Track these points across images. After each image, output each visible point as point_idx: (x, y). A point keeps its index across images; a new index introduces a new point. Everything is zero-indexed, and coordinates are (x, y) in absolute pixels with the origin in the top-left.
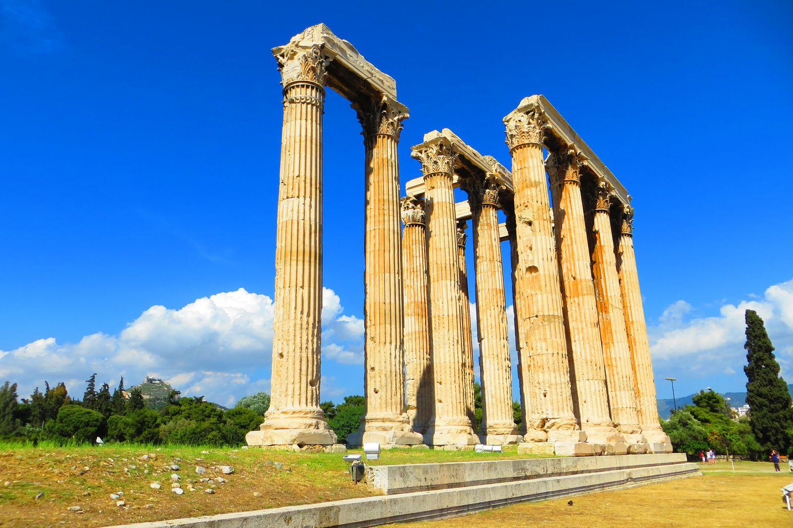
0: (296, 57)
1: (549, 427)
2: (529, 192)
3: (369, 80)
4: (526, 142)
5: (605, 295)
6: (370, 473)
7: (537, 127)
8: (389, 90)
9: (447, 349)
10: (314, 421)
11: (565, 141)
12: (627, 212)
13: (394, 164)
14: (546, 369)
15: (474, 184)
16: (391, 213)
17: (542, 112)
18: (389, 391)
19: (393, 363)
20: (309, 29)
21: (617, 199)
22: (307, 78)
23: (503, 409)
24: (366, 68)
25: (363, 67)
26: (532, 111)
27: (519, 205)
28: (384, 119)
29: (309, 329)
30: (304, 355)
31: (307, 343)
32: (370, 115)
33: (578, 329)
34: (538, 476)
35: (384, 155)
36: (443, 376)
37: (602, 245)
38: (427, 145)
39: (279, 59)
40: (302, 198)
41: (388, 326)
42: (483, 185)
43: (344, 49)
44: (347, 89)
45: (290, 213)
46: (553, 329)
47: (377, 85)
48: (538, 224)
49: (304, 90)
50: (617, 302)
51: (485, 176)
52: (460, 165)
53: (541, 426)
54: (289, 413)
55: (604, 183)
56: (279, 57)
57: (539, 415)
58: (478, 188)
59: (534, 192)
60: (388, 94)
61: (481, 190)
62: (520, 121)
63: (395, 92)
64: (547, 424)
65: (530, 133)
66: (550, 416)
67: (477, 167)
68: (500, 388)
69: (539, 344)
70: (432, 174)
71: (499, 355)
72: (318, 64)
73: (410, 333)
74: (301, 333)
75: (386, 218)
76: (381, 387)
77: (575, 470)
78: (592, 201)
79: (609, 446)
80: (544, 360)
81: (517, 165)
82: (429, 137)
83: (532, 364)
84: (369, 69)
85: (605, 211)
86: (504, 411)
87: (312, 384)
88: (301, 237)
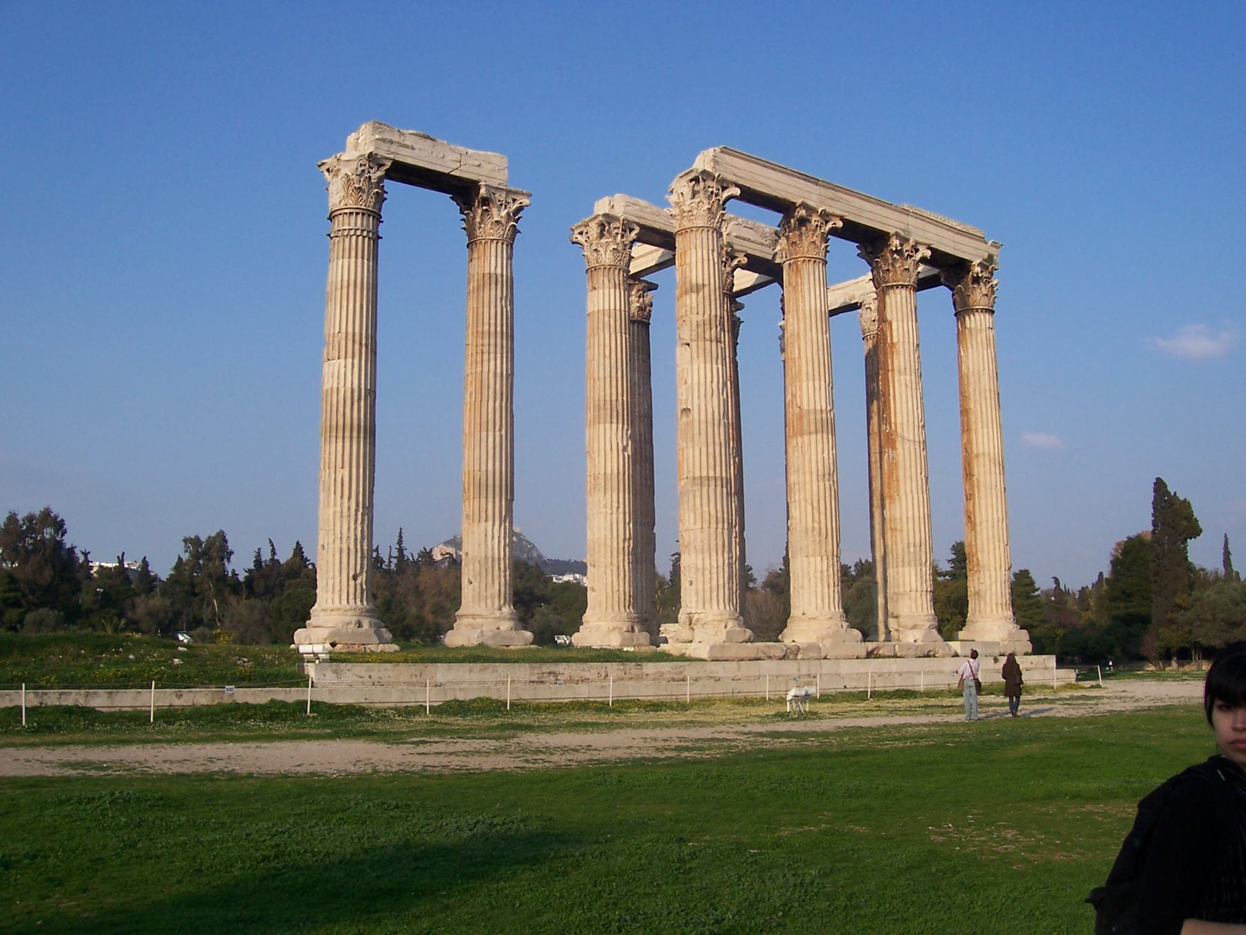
5: (893, 421)
9: (602, 520)
10: (355, 619)
13: (500, 279)
14: (692, 550)
16: (492, 349)
33: (799, 484)
36: (596, 557)
37: (895, 340)
40: (342, 360)
41: (483, 500)
74: (341, 522)
75: (486, 356)
76: (474, 576)
78: (883, 271)
80: (692, 537)
88: (341, 409)
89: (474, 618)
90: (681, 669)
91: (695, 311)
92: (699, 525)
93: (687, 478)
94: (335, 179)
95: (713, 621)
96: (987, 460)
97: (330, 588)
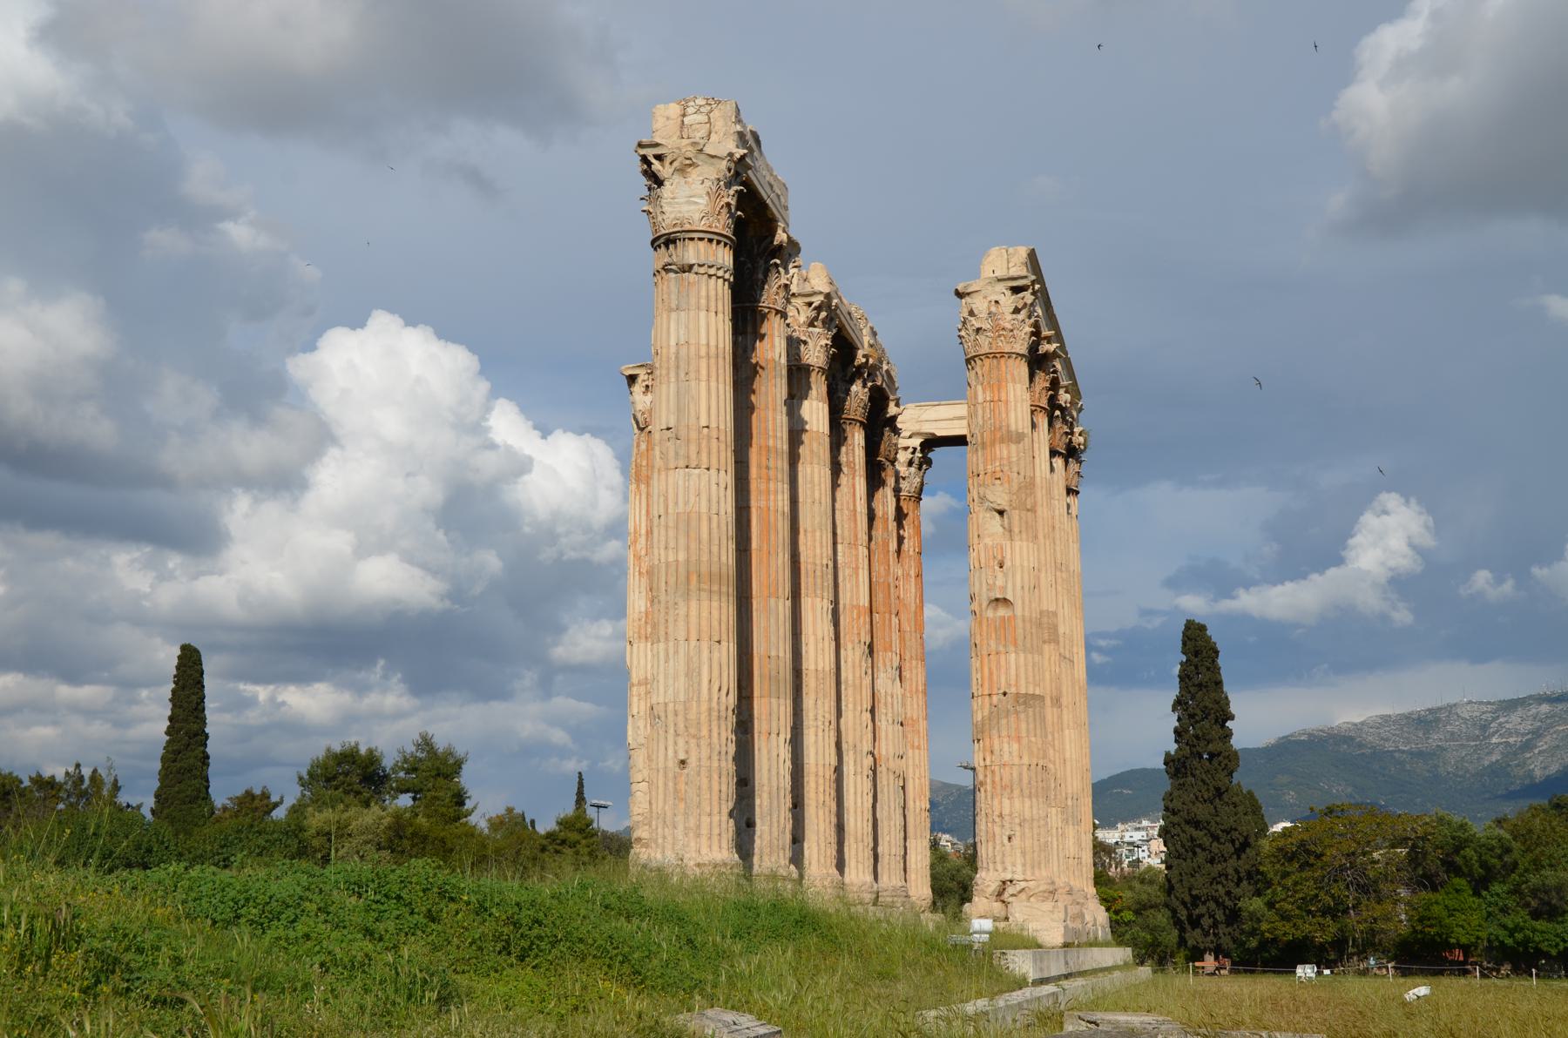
1: (1012, 895)
2: (1005, 453)
12: (1079, 445)
14: (1017, 792)
23: (860, 854)
27: (982, 473)
46: (1031, 719)
48: (1017, 517)
51: (854, 357)
56: (653, 161)
57: (996, 873)
59: (1014, 454)
62: (997, 302)
64: (1010, 890)
66: (1017, 877)
68: (856, 812)
69: (1006, 746)
71: (858, 745)
80: (1015, 775)
81: (984, 392)
93: (1005, 694)
94: (677, 178)
95: (1045, 892)
97: (704, 831)
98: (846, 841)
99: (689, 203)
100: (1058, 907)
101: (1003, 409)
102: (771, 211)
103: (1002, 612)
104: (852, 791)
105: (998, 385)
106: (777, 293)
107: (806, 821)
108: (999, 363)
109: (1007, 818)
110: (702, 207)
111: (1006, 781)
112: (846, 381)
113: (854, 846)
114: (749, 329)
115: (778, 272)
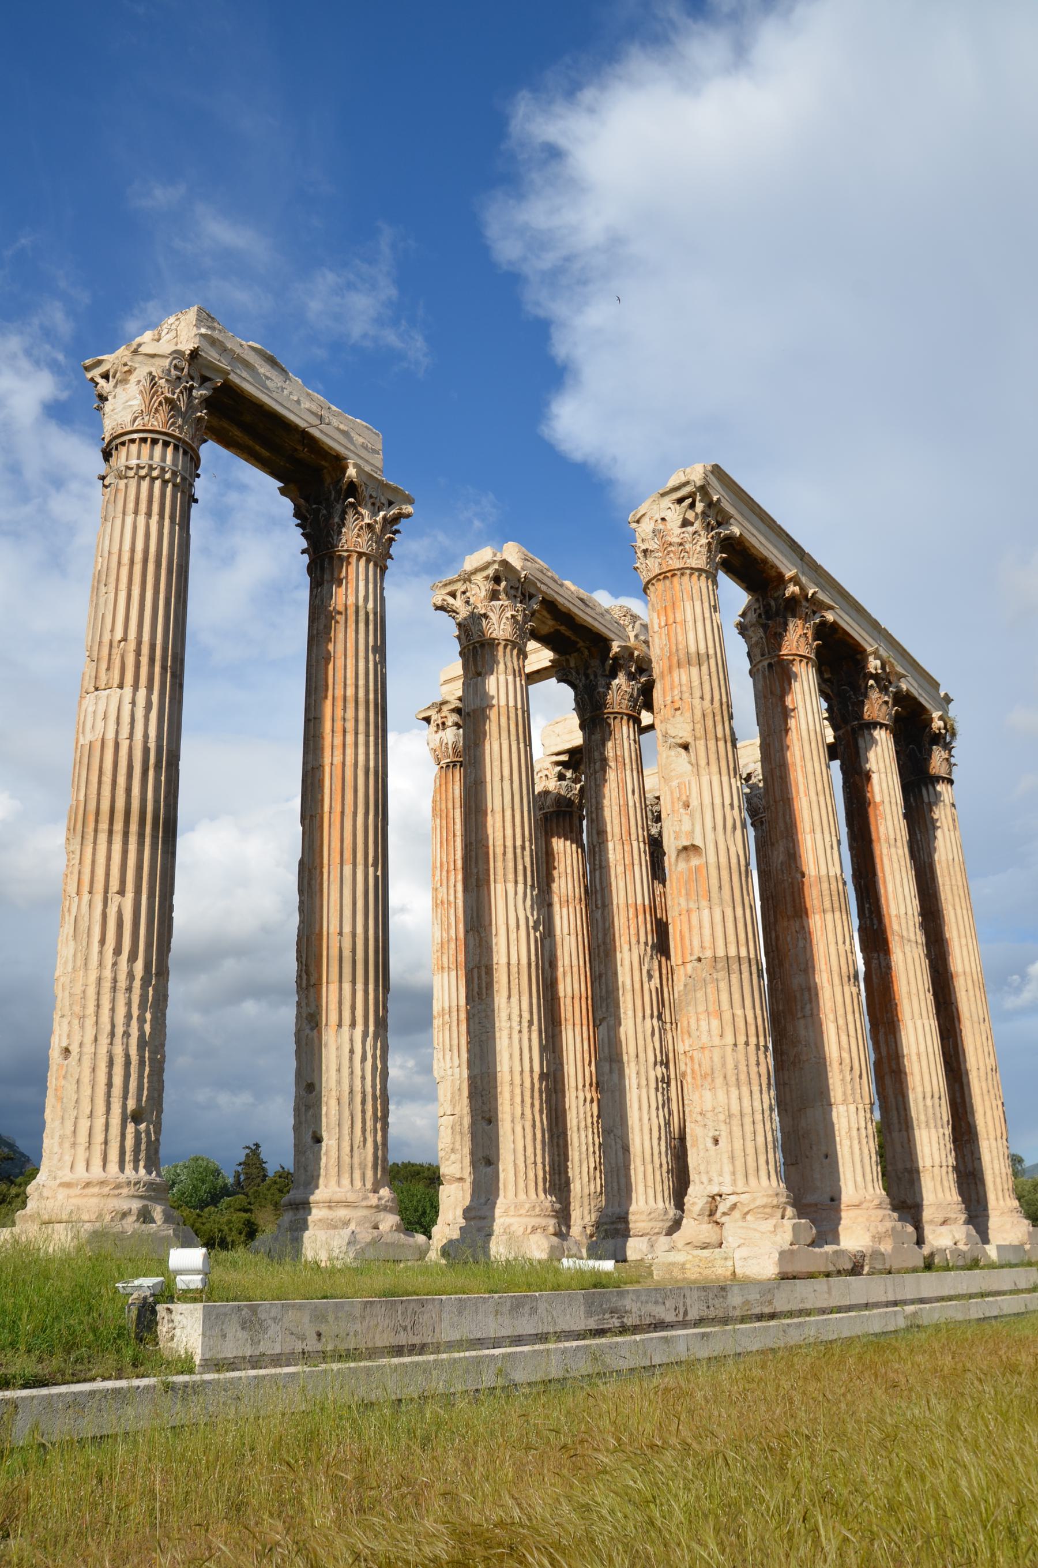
0: (133, 378)
1: (724, 1214)
2: (684, 679)
3: (313, 431)
4: (678, 564)
6: (166, 1320)
7: (702, 533)
8: (363, 453)
10: (136, 1205)
11: (777, 568)
12: (939, 729)
15: (587, 668)
17: (715, 498)
18: (346, 1138)
19: (358, 1072)
20: (172, 319)
21: (915, 699)
22: (156, 423)
24: (306, 404)
25: (298, 402)
26: (688, 498)
28: (350, 517)
29: (134, 989)
30: (118, 1051)
31: (128, 1024)
32: (319, 510)
34: (659, 1325)
35: (349, 597)
38: (467, 578)
39: (97, 384)
40: (128, 691)
42: (605, 670)
43: (252, 361)
44: (265, 453)
45: (100, 724)
47: (333, 442)
49: (146, 448)
50: (912, 929)
52: (549, 625)
53: (707, 1213)
54: (77, 1185)
55: (878, 663)
57: (702, 1187)
58: (596, 677)
60: (360, 462)
61: (602, 681)
62: (663, 519)
63: (378, 460)
64: (723, 1208)
65: (687, 546)
66: (725, 1190)
67: (590, 630)
68: (641, 1130)
69: (703, 1024)
70: (478, 642)
71: (642, 1055)
72: (181, 392)
73: (447, 1008)
74: (113, 1001)
75: (350, 738)
77: (767, 1310)
79: (876, 1254)
81: (659, 618)
82: (471, 562)
83: (689, 1071)
84: (314, 408)
85: (887, 726)
86: (650, 1183)
87: (137, 1117)
88: (122, 780)
89: (330, 1207)
90: (769, 1297)
91: (697, 694)
92: (729, 1039)
93: (699, 960)
95: (764, 1207)
96: (970, 982)
97: (82, 1138)
98: (632, 1167)
99: (124, 408)
100: (783, 1225)
101: (679, 630)
102: (323, 443)
103: (695, 862)
104: (636, 1106)
105: (670, 607)
106: (359, 536)
107: (501, 1139)
108: (672, 583)
109: (709, 1115)
110: (135, 409)
111: (706, 1067)
112: (606, 676)
113: (640, 1169)
114: (327, 577)
115: (357, 512)
